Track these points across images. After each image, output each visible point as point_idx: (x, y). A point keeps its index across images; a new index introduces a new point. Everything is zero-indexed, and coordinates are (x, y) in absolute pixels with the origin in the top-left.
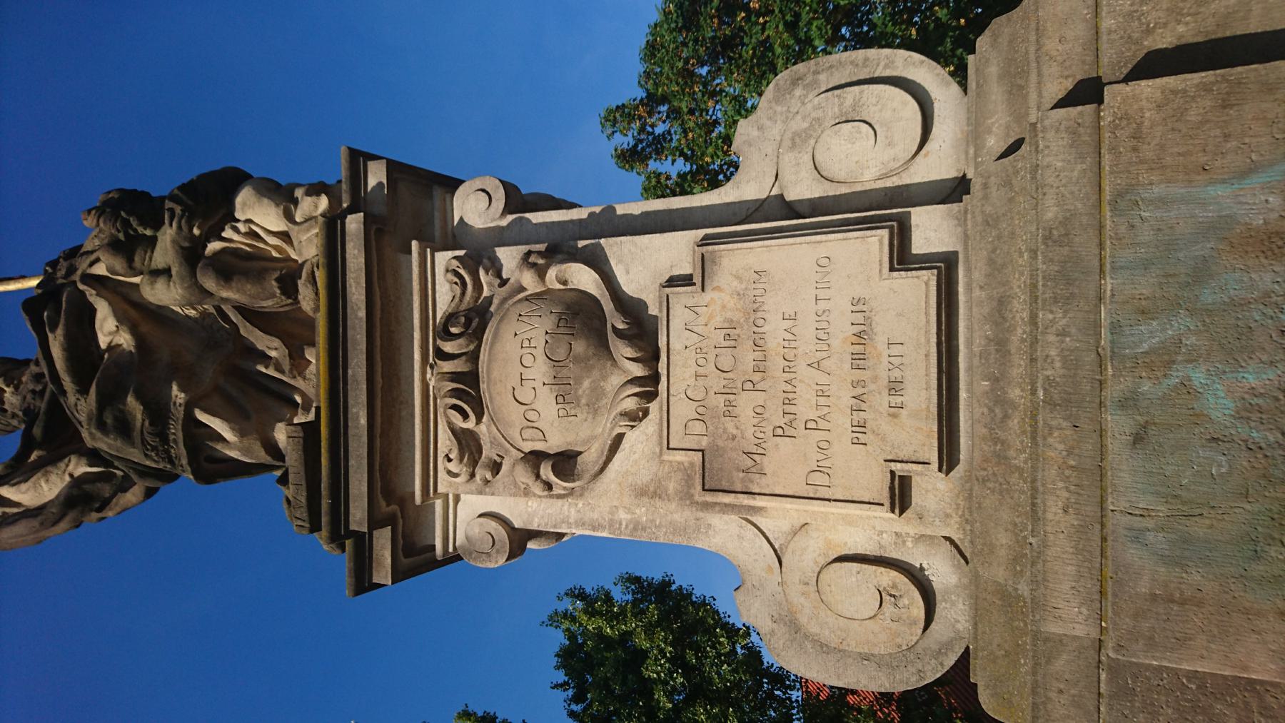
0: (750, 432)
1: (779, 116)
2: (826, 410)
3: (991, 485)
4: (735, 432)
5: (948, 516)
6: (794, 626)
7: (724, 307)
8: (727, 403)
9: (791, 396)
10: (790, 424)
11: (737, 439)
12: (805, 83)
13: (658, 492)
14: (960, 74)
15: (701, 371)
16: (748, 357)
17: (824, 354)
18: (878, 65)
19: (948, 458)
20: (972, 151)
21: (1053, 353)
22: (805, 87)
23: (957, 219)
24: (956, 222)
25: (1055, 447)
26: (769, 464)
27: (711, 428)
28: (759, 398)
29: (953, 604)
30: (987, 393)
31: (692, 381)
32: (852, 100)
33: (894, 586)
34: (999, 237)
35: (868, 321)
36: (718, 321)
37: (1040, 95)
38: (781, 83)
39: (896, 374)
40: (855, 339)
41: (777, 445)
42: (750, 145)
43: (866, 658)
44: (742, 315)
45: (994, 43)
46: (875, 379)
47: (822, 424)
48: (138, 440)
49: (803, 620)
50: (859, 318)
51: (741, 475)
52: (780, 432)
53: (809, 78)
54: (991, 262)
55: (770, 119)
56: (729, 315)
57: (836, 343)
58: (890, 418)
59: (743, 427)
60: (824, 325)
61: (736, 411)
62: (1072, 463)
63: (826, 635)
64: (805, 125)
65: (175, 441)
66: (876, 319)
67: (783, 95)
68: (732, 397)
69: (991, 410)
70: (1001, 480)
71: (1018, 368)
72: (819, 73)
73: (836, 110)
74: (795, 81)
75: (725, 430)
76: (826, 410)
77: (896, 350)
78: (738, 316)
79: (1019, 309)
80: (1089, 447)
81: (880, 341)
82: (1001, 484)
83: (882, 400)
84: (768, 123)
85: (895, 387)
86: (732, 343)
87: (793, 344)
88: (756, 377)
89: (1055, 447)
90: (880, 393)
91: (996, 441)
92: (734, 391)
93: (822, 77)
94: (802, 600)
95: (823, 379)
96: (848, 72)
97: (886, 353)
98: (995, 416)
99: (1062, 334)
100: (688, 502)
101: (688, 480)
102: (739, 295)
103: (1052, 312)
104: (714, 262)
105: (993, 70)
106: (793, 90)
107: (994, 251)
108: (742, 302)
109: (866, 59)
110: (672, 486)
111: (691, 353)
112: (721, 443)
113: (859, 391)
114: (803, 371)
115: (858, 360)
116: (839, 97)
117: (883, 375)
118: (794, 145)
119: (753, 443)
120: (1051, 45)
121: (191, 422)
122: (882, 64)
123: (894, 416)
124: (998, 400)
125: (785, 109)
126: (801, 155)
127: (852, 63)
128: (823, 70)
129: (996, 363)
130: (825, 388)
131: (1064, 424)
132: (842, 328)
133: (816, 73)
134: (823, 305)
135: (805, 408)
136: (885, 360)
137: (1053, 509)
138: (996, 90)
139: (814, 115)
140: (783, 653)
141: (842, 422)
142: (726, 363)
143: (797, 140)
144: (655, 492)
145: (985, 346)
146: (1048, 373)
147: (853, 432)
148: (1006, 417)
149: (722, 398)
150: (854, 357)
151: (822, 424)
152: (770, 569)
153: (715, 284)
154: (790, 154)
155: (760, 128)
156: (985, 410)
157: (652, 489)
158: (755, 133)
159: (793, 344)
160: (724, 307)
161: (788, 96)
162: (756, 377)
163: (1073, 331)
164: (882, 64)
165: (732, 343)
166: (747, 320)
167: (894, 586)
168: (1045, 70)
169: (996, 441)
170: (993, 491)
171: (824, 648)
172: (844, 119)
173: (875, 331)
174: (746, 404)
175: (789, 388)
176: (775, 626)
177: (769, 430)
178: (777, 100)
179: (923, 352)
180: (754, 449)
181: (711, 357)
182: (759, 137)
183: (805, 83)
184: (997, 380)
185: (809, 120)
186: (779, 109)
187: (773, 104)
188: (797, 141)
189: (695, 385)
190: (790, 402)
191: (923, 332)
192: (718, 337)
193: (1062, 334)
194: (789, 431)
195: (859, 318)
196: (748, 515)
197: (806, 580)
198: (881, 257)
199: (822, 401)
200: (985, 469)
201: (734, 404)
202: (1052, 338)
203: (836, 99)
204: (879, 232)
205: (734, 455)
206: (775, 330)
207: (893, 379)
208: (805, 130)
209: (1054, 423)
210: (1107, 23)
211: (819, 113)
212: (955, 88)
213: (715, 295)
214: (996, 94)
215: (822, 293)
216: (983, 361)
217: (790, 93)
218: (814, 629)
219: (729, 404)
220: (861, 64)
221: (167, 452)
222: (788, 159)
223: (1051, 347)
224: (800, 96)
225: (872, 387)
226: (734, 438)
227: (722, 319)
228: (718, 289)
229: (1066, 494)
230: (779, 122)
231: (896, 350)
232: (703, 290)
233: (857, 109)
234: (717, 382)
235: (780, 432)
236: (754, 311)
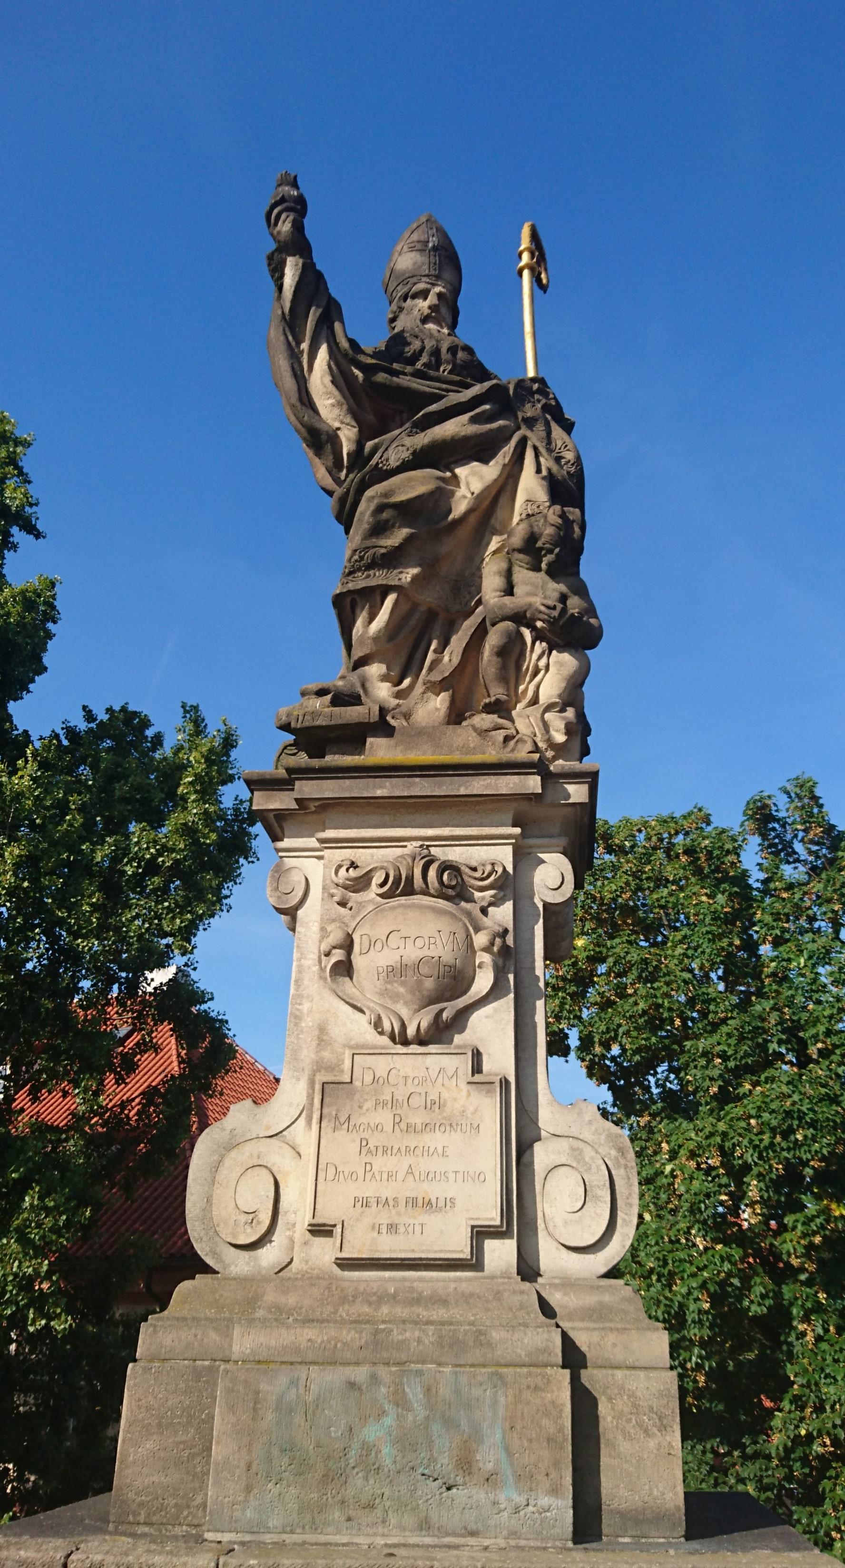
0: (363, 1120)
2: (378, 1178)
3: (326, 1293)
4: (365, 1108)
5: (307, 1262)
6: (231, 1146)
7: (455, 1099)
9: (389, 1152)
10: (369, 1151)
14: (613, 1273)
15: (410, 1081)
16: (417, 1119)
17: (417, 1178)
19: (345, 1264)
20: (557, 1281)
22: (617, 1159)
25: (348, 1335)
26: (341, 1134)
27: (367, 1089)
28: (389, 1127)
29: (248, 1263)
31: (402, 1073)
33: (259, 1223)
35: (439, 1210)
36: (445, 1095)
37: (581, 1329)
39: (402, 1229)
40: (426, 1201)
42: (578, 1114)
43: (209, 1200)
45: (628, 1300)
46: (399, 1214)
47: (369, 1175)
48: (368, 543)
49: (234, 1154)
50: (441, 1203)
51: (334, 1113)
52: (364, 1144)
54: (471, 1295)
56: (449, 1104)
57: (425, 1186)
60: (438, 1178)
61: (379, 1108)
62: (339, 1345)
63: (223, 1172)
65: (368, 576)
68: (390, 1105)
69: (375, 1294)
71: (401, 1312)
74: (621, 1151)
75: (366, 1100)
76: (378, 1178)
77: (418, 1229)
78: (448, 1110)
79: (439, 1313)
80: (348, 1355)
81: (424, 1218)
83: (384, 1219)
85: (392, 1228)
86: (429, 1106)
87: (426, 1154)
88: (403, 1125)
89: (348, 1335)
93: (622, 1171)
94: (247, 1154)
95: (400, 1176)
97: (416, 1222)
101: (330, 1068)
104: (488, 1092)
105: (607, 1298)
107: (479, 1297)
109: (631, 1205)
110: (326, 1054)
112: (357, 1096)
113: (391, 1203)
115: (412, 1202)
118: (573, 1149)
120: (612, 1338)
121: (385, 591)
122: (626, 1217)
123: (373, 1227)
124: (381, 1298)
127: (630, 1194)
131: (363, 1341)
132: (435, 1191)
133: (626, 1167)
134: (452, 1176)
135: (380, 1163)
136: (411, 1221)
137: (309, 1333)
139: (594, 1166)
141: (369, 1190)
142: (416, 1101)
143: (577, 1153)
144: (322, 1040)
146: (395, 1332)
148: (370, 1304)
149: (389, 1098)
151: (369, 1175)
152: (268, 1128)
153: (472, 1093)
155: (590, 1123)
158: (587, 1118)
159: (426, 1154)
160: (455, 1099)
162: (403, 1125)
163: (421, 1348)
165: (429, 1106)
166: (445, 1118)
167: (259, 1223)
168: (596, 1333)
169: (355, 1297)
170: (323, 1294)
171: (216, 1167)
174: (384, 1117)
175: (395, 1151)
176: (228, 1132)
177: (365, 1135)
178: (609, 1136)
180: (352, 1123)
181: (419, 1089)
186: (603, 1137)
188: (577, 1153)
190: (385, 1152)
192: (433, 1096)
194: (364, 1152)
195: (441, 1203)
196: (306, 1111)
199: (385, 1176)
202: (417, 1333)
204: (499, 1218)
205: (348, 1108)
206: (436, 1140)
208: (583, 1159)
210: (619, 1374)
211: (594, 1170)
212: (603, 1270)
213: (464, 1092)
214: (590, 1300)
215: (460, 1176)
218: (227, 1162)
219: (385, 1104)
221: (359, 570)
223: (411, 1334)
225: (393, 1212)
226: (360, 1107)
228: (469, 1095)
229: (319, 1341)
231: (418, 1229)
232: (469, 1083)
234: (401, 1094)
235: (364, 1143)
236: (451, 1125)
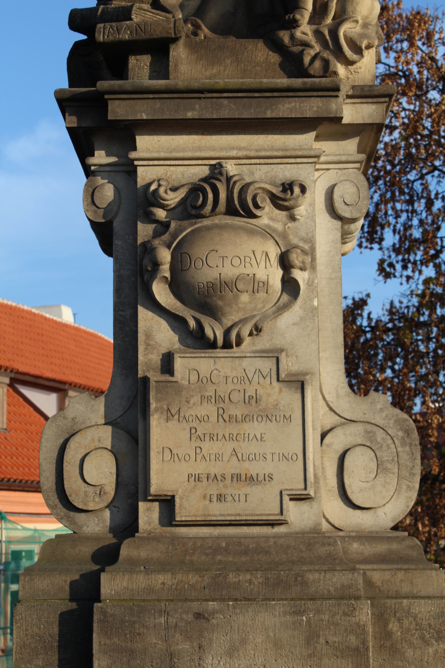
1: (387, 422)
4: (192, 402)
7: (269, 395)
8: (210, 398)
11: (187, 404)
12: (405, 438)
13: (149, 347)
15: (230, 380)
21: (241, 578)
24: (312, 528)
28: (213, 418)
34: (301, 551)
39: (229, 498)
40: (249, 475)
41: (184, 429)
44: (264, 407)
46: (225, 487)
47: (199, 457)
50: (261, 478)
51: (165, 407)
52: (193, 431)
53: (408, 441)
55: (387, 416)
56: (264, 399)
57: (246, 465)
59: (194, 408)
60: (257, 458)
64: (379, 439)
66: (260, 487)
67: (400, 425)
68: (213, 400)
69: (210, 548)
70: (174, 552)
72: (410, 446)
73: (385, 458)
76: (208, 459)
78: (263, 404)
82: (171, 552)
84: (384, 415)
85: (220, 498)
86: (247, 401)
90: (217, 489)
94: (89, 438)
96: (408, 464)
97: (240, 492)
99: (250, 582)
100: (144, 368)
102: (277, 405)
103: (261, 577)
106: (402, 430)
108: (272, 407)
111: (240, 373)
112: (184, 393)
113: (219, 478)
114: (230, 446)
116: (393, 460)
117: (229, 491)
123: (205, 497)
125: (391, 425)
128: (411, 449)
130: (220, 459)
134: (269, 457)
140: (54, 425)
153: (283, 389)
154: (362, 430)
156: (210, 545)
157: (151, 342)
161: (399, 427)
164: (410, 484)
165: (247, 401)
166: (260, 410)
175: (220, 437)
179: (241, 513)
180: (182, 415)
182: (376, 409)
183: (405, 438)
185: (382, 442)
187: (395, 418)
189: (219, 376)
192: (250, 392)
193: (250, 582)
195: (261, 478)
197: (101, 441)
198: (295, 490)
199: (213, 457)
200: (179, 545)
201: (209, 402)
203: (391, 458)
207: (226, 496)
213: (277, 389)
217: (400, 428)
224: (397, 435)
225: (221, 484)
226: (188, 402)
227: (261, 394)
228: (281, 391)
230: (384, 422)
231: (243, 498)
235: (193, 431)
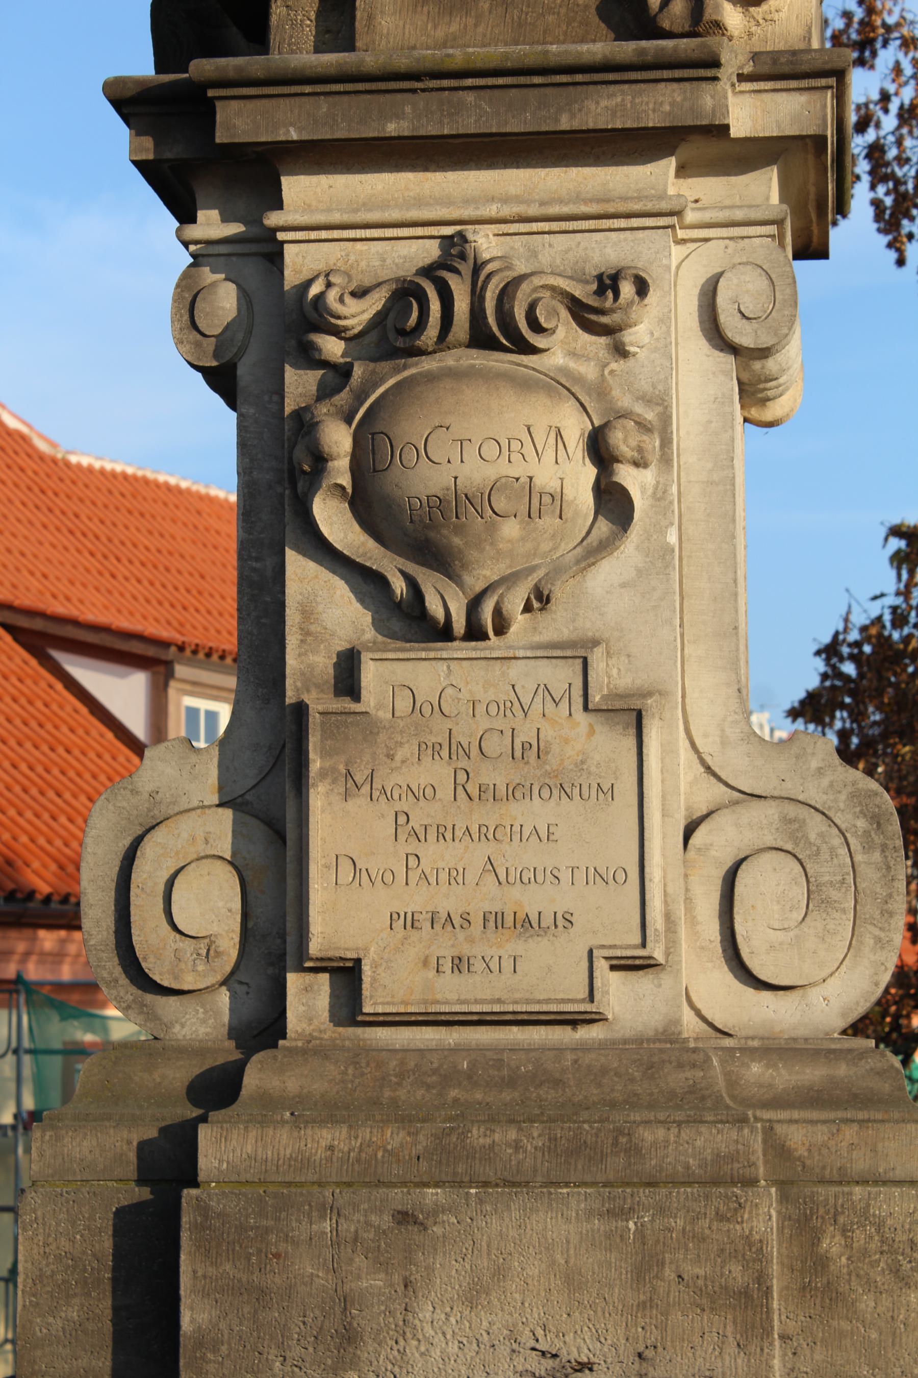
1: (832, 797)
4: (398, 758)
8: (437, 747)
11: (389, 761)
12: (873, 833)
18: (881, 929)
23: (665, 1031)
24: (661, 1030)
28: (445, 792)
30: (455, 1067)
32: (836, 898)
38: (878, 800)
39: (479, 966)
40: (521, 916)
41: (383, 816)
46: (471, 940)
47: (414, 876)
50: (547, 921)
52: (401, 818)
53: (878, 839)
55: (831, 785)
57: (516, 892)
58: (423, 958)
64: (812, 837)
66: (544, 942)
68: (445, 753)
69: (435, 1072)
72: (883, 851)
76: (433, 880)
81: (516, 946)
84: (825, 782)
85: (459, 964)
90: (453, 946)
91: (401, 1076)
92: (454, 757)
97: (501, 952)
98: (429, 1076)
106: (865, 816)
112: (382, 737)
113: (457, 921)
117: (477, 950)
119: (385, 783)
123: (425, 963)
125: (842, 805)
126: (773, 831)
128: (886, 857)
129: (489, 1076)
136: (495, 952)
138: (816, 1072)
145: (508, 1065)
147: (406, 913)
150: (499, 916)
154: (776, 817)
156: (435, 1065)
161: (858, 809)
172: (812, 888)
173: (530, 940)
175: (459, 834)
179: (504, 997)
183: (873, 833)
184: (470, 1078)
185: (818, 842)
187: (850, 789)
189: (459, 699)
191: (527, 995)
195: (547, 921)
199: (444, 876)
201: (436, 756)
203: (839, 878)
209: (421, 1137)
216: (491, 1063)
217: (861, 812)
220: (885, 907)
222: (770, 812)
224: (855, 826)
225: (461, 935)
226: (391, 757)
230: (825, 797)
231: (507, 965)
233: (824, 905)
235: (402, 819)
